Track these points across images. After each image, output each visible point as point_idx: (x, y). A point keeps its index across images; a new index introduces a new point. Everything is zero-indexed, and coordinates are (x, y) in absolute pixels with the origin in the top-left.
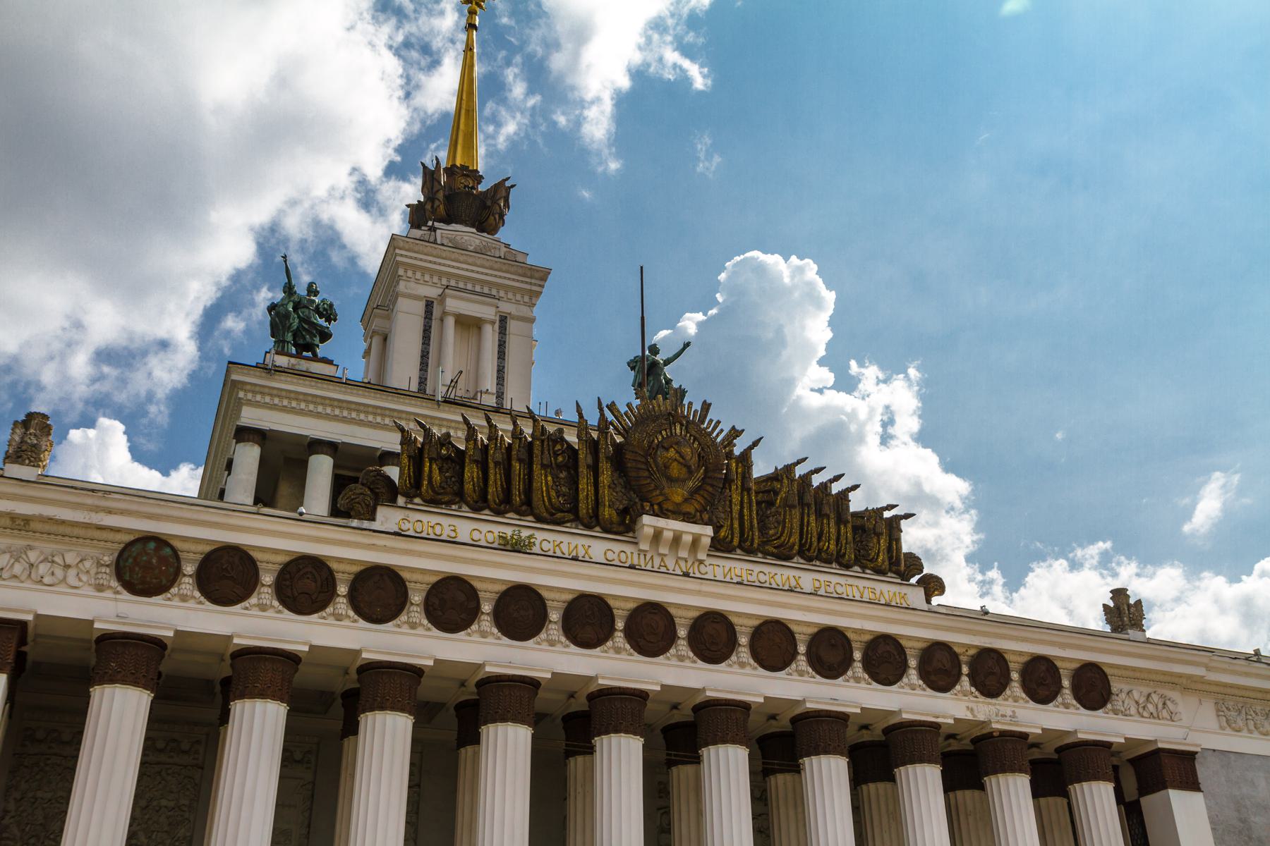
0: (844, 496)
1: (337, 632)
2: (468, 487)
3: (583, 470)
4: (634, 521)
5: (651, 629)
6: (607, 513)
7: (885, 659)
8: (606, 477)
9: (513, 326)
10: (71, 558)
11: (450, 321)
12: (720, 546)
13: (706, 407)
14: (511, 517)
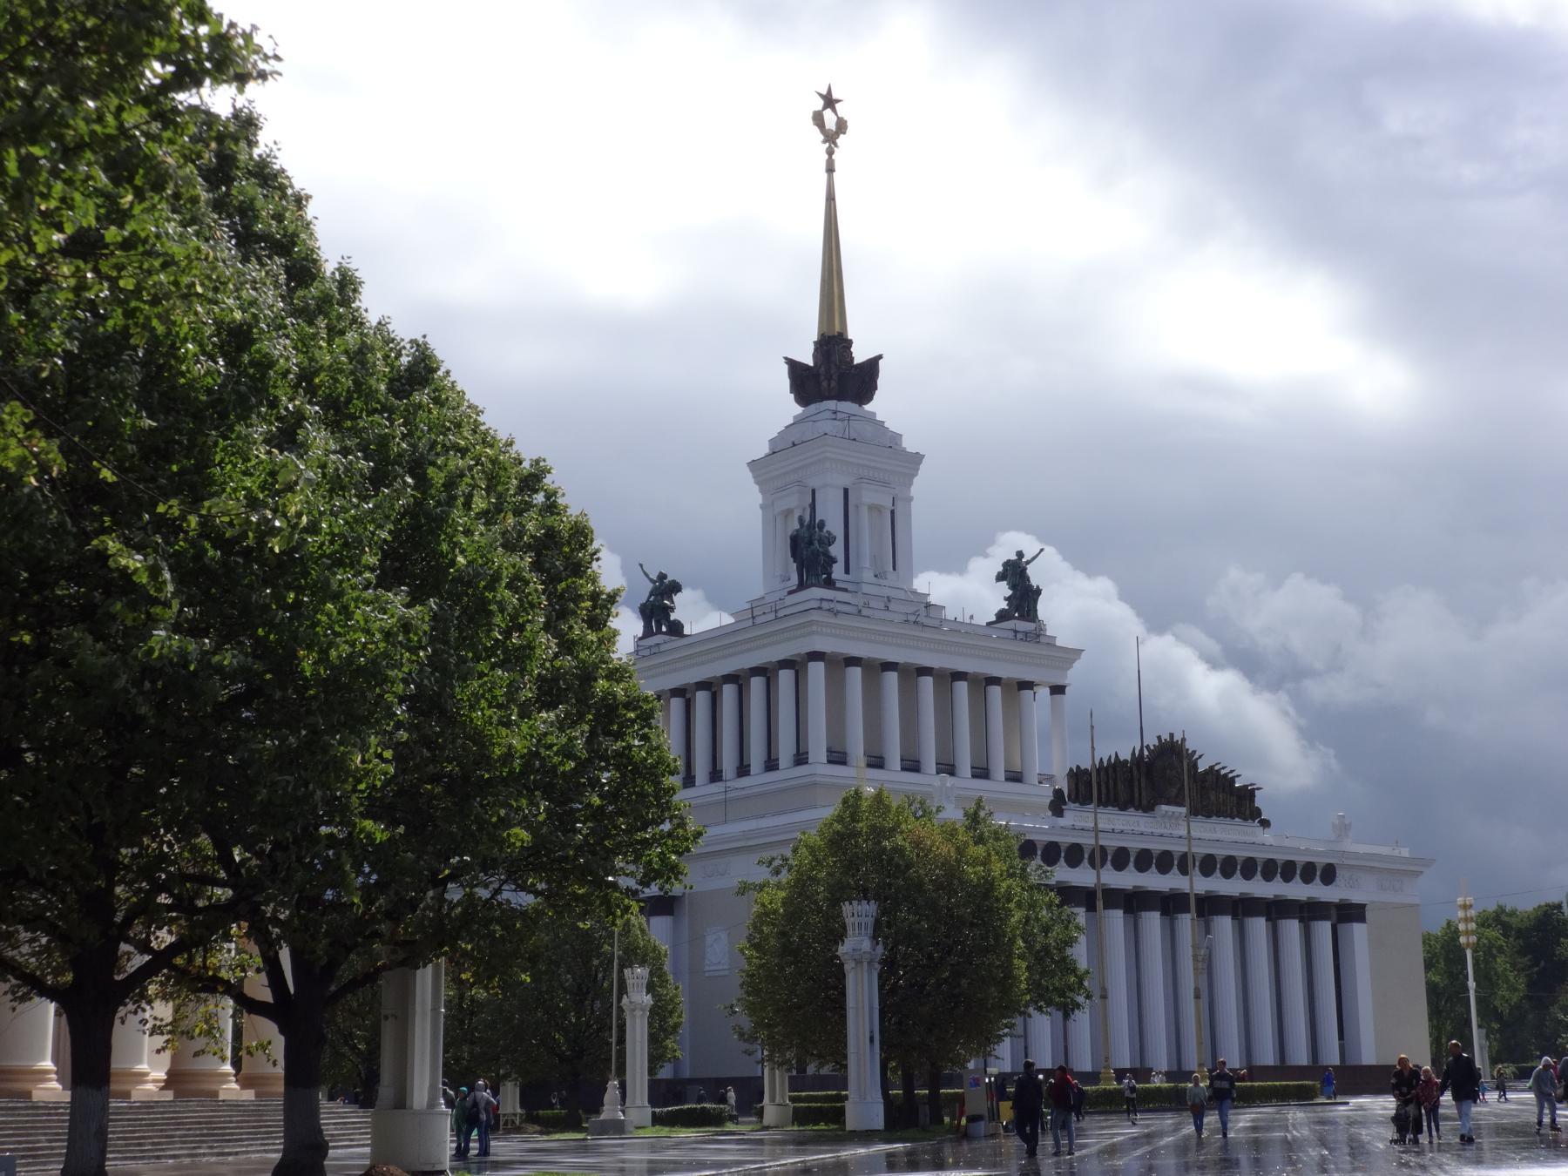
5: (1164, 862)
6: (1144, 802)
7: (1249, 868)
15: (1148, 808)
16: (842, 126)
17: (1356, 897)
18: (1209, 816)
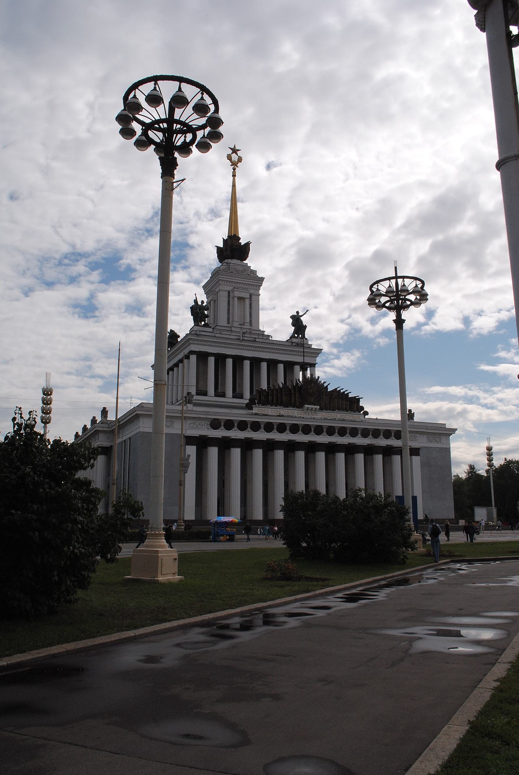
0: (348, 394)
1: (248, 434)
3: (293, 395)
6: (297, 404)
7: (354, 432)
8: (297, 397)
9: (254, 298)
10: (203, 424)
11: (236, 299)
12: (321, 409)
13: (319, 377)
14: (278, 407)
15: (300, 406)
16: (240, 160)
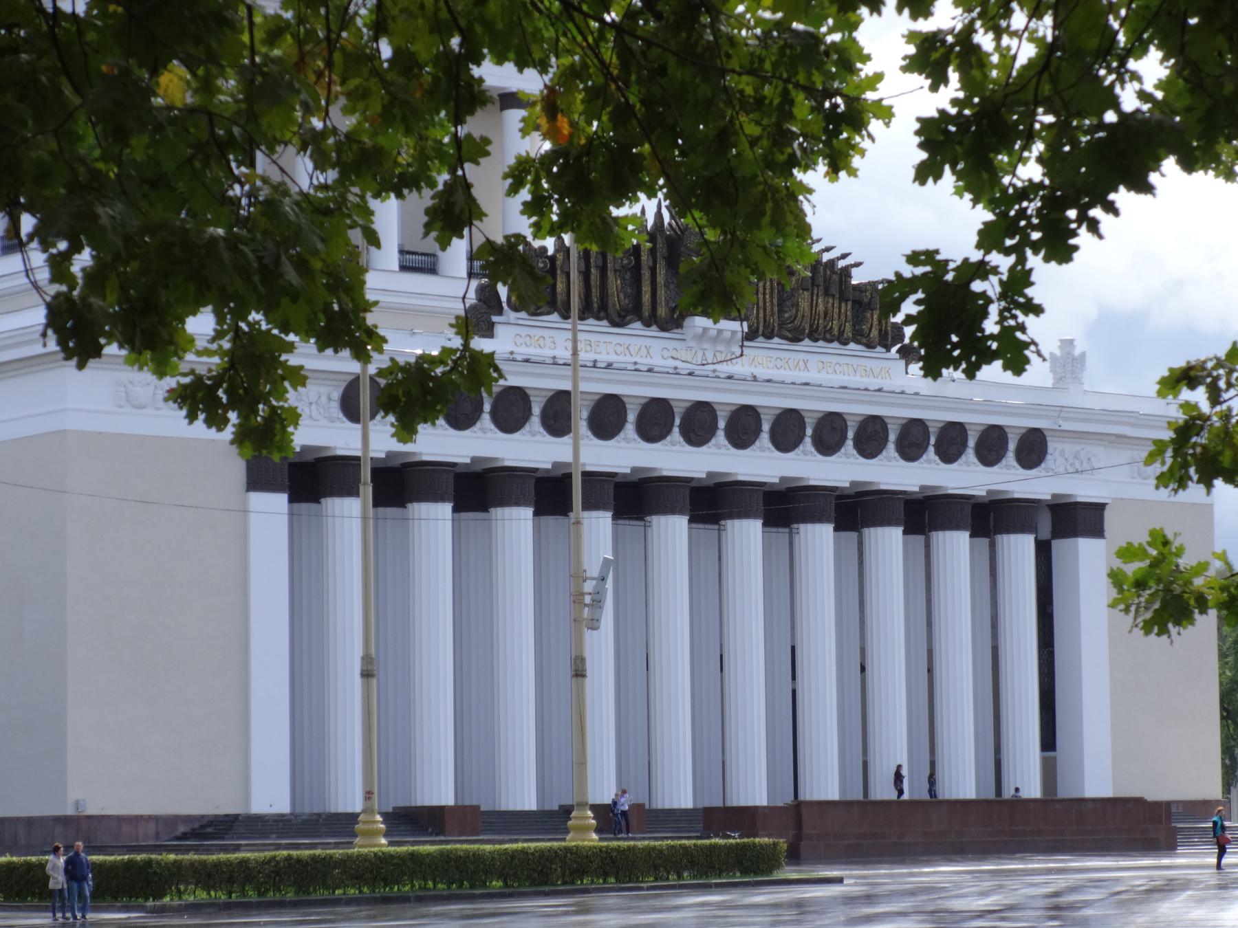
2: (559, 304)
3: (646, 274)
4: (683, 317)
5: (698, 424)
6: (662, 311)
8: (661, 279)
15: (671, 322)
17: (1084, 491)
18: (796, 339)
